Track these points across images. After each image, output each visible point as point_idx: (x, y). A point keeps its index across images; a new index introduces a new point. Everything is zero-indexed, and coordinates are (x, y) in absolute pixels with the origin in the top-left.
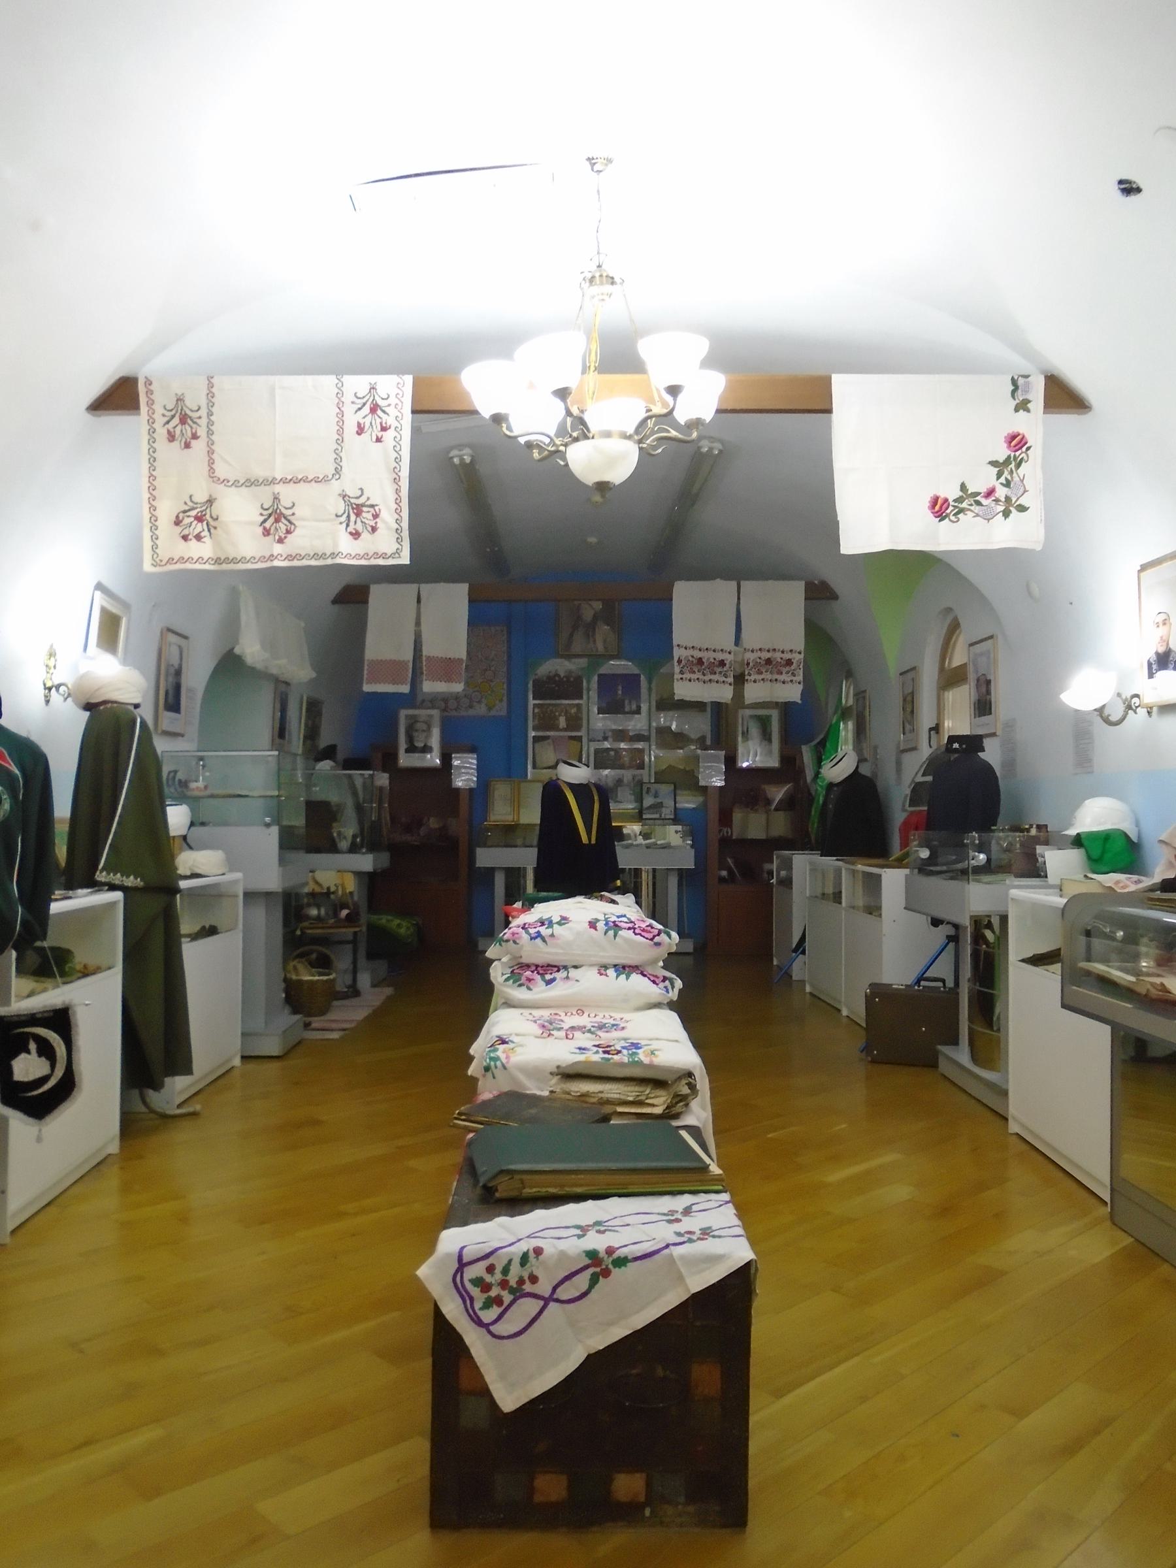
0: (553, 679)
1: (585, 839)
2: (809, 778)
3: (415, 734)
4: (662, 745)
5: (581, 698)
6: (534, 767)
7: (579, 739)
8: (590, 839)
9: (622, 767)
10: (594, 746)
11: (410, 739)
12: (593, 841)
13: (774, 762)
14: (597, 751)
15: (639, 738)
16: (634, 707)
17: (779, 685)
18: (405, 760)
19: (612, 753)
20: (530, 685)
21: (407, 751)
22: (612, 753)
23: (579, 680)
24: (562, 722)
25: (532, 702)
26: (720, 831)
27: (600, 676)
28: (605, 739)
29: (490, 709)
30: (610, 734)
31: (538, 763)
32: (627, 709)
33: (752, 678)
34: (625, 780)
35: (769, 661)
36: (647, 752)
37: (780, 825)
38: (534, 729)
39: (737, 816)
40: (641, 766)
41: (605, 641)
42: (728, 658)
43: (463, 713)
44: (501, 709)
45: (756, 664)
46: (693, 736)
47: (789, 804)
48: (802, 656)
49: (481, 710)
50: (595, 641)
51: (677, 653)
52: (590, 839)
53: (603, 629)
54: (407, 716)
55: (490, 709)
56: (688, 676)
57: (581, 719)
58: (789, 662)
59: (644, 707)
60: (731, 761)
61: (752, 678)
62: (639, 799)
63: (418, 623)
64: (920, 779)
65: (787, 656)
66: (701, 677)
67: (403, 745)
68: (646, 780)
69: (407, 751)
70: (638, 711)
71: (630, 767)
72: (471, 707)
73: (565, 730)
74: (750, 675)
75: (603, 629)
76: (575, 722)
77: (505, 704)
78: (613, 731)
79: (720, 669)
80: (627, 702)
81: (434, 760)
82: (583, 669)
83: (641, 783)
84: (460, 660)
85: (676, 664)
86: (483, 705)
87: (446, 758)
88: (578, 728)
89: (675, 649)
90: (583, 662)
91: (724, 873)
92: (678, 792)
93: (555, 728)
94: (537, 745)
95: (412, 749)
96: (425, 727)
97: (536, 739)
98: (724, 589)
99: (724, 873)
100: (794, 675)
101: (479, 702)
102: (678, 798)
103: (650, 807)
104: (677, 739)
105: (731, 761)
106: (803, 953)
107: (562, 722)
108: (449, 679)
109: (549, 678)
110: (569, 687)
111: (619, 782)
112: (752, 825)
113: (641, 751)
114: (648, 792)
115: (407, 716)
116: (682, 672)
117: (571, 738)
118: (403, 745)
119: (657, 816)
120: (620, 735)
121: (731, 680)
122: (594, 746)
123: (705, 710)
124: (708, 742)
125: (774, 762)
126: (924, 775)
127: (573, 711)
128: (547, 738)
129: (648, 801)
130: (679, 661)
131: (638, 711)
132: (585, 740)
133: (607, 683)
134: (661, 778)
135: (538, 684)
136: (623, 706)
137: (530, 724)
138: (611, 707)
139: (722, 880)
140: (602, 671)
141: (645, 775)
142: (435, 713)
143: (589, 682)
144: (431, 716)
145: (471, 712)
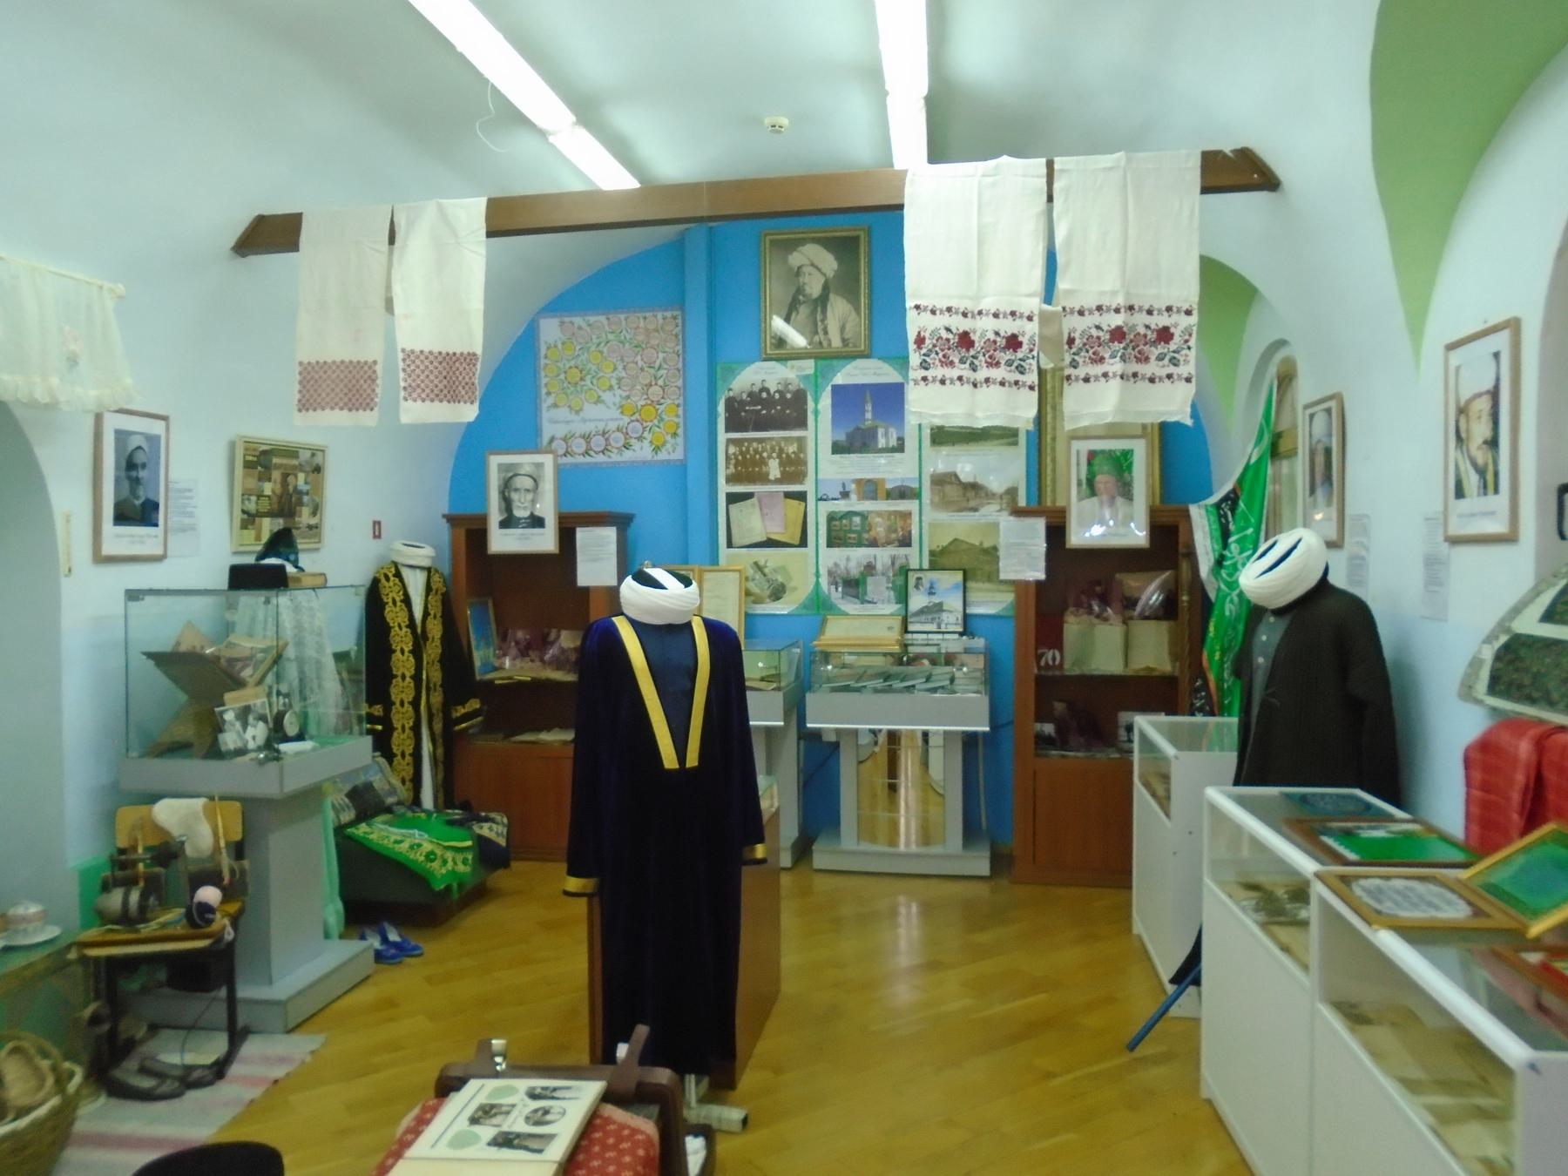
0: (757, 396)
1: (669, 759)
2: (1204, 569)
3: (514, 496)
4: (944, 504)
5: (801, 423)
6: (730, 545)
7: (801, 496)
9: (873, 543)
10: (826, 508)
11: (507, 504)
12: (692, 760)
13: (1137, 535)
14: (831, 518)
15: (903, 493)
16: (893, 442)
17: (1144, 385)
18: (502, 542)
19: (857, 520)
20: (721, 408)
21: (505, 524)
22: (857, 520)
23: (800, 397)
24: (774, 469)
25: (722, 436)
26: (1039, 657)
27: (837, 390)
28: (845, 495)
29: (657, 449)
30: (853, 486)
31: (736, 540)
32: (882, 442)
33: (1081, 372)
34: (879, 567)
35: (1118, 334)
36: (915, 518)
37: (1152, 650)
38: (729, 480)
39: (1073, 626)
40: (906, 542)
41: (842, 329)
42: (1029, 331)
43: (615, 457)
44: (673, 452)
45: (1092, 342)
46: (996, 484)
47: (1168, 609)
48: (1194, 319)
49: (642, 452)
50: (826, 332)
51: (914, 324)
53: (838, 307)
54: (500, 465)
55: (657, 449)
56: (938, 372)
57: (805, 464)
58: (1165, 335)
59: (911, 444)
60: (1056, 533)
61: (1081, 372)
62: (903, 598)
63: (388, 287)
64: (1530, 624)
65: (1160, 321)
66: (967, 373)
67: (495, 518)
68: (914, 564)
69: (505, 524)
70: (900, 448)
71: (888, 543)
72: (627, 446)
73: (778, 481)
74: (1074, 364)
75: (838, 307)
76: (794, 469)
77: (680, 440)
78: (859, 482)
79: (1009, 355)
80: (881, 431)
81: (545, 541)
82: (807, 377)
83: (905, 571)
84: (471, 358)
85: (912, 346)
86: (646, 442)
87: (567, 536)
88: (799, 477)
89: (911, 315)
90: (809, 366)
91: (1049, 728)
92: (970, 584)
93: (763, 479)
94: (734, 508)
95: (508, 522)
96: (528, 483)
97: (733, 499)
98: (1017, 175)
99: (1049, 728)
100: (1174, 362)
101: (640, 439)
102: (972, 597)
103: (922, 612)
104: (972, 493)
105: (1056, 533)
106: (1197, 982)
107: (774, 469)
108: (454, 397)
109: (750, 394)
110: (786, 411)
111: (870, 568)
112: (1102, 646)
113: (906, 516)
114: (917, 587)
115: (500, 465)
116: (925, 366)
117: (788, 495)
118: (495, 518)
119: (933, 627)
120: (870, 489)
121: (1032, 378)
122: (826, 508)
123: (1015, 444)
124: (1022, 503)
125: (1137, 535)
126: (1549, 616)
127: (792, 449)
128: (749, 496)
129: (918, 601)
130: (920, 341)
131: (900, 448)
132: (811, 498)
133: (846, 398)
134: (939, 560)
135: (731, 404)
136: (874, 437)
138: (855, 442)
139: (1042, 741)
140: (840, 379)
141: (914, 557)
142: (547, 460)
143: (816, 402)
144: (539, 466)
145: (628, 455)
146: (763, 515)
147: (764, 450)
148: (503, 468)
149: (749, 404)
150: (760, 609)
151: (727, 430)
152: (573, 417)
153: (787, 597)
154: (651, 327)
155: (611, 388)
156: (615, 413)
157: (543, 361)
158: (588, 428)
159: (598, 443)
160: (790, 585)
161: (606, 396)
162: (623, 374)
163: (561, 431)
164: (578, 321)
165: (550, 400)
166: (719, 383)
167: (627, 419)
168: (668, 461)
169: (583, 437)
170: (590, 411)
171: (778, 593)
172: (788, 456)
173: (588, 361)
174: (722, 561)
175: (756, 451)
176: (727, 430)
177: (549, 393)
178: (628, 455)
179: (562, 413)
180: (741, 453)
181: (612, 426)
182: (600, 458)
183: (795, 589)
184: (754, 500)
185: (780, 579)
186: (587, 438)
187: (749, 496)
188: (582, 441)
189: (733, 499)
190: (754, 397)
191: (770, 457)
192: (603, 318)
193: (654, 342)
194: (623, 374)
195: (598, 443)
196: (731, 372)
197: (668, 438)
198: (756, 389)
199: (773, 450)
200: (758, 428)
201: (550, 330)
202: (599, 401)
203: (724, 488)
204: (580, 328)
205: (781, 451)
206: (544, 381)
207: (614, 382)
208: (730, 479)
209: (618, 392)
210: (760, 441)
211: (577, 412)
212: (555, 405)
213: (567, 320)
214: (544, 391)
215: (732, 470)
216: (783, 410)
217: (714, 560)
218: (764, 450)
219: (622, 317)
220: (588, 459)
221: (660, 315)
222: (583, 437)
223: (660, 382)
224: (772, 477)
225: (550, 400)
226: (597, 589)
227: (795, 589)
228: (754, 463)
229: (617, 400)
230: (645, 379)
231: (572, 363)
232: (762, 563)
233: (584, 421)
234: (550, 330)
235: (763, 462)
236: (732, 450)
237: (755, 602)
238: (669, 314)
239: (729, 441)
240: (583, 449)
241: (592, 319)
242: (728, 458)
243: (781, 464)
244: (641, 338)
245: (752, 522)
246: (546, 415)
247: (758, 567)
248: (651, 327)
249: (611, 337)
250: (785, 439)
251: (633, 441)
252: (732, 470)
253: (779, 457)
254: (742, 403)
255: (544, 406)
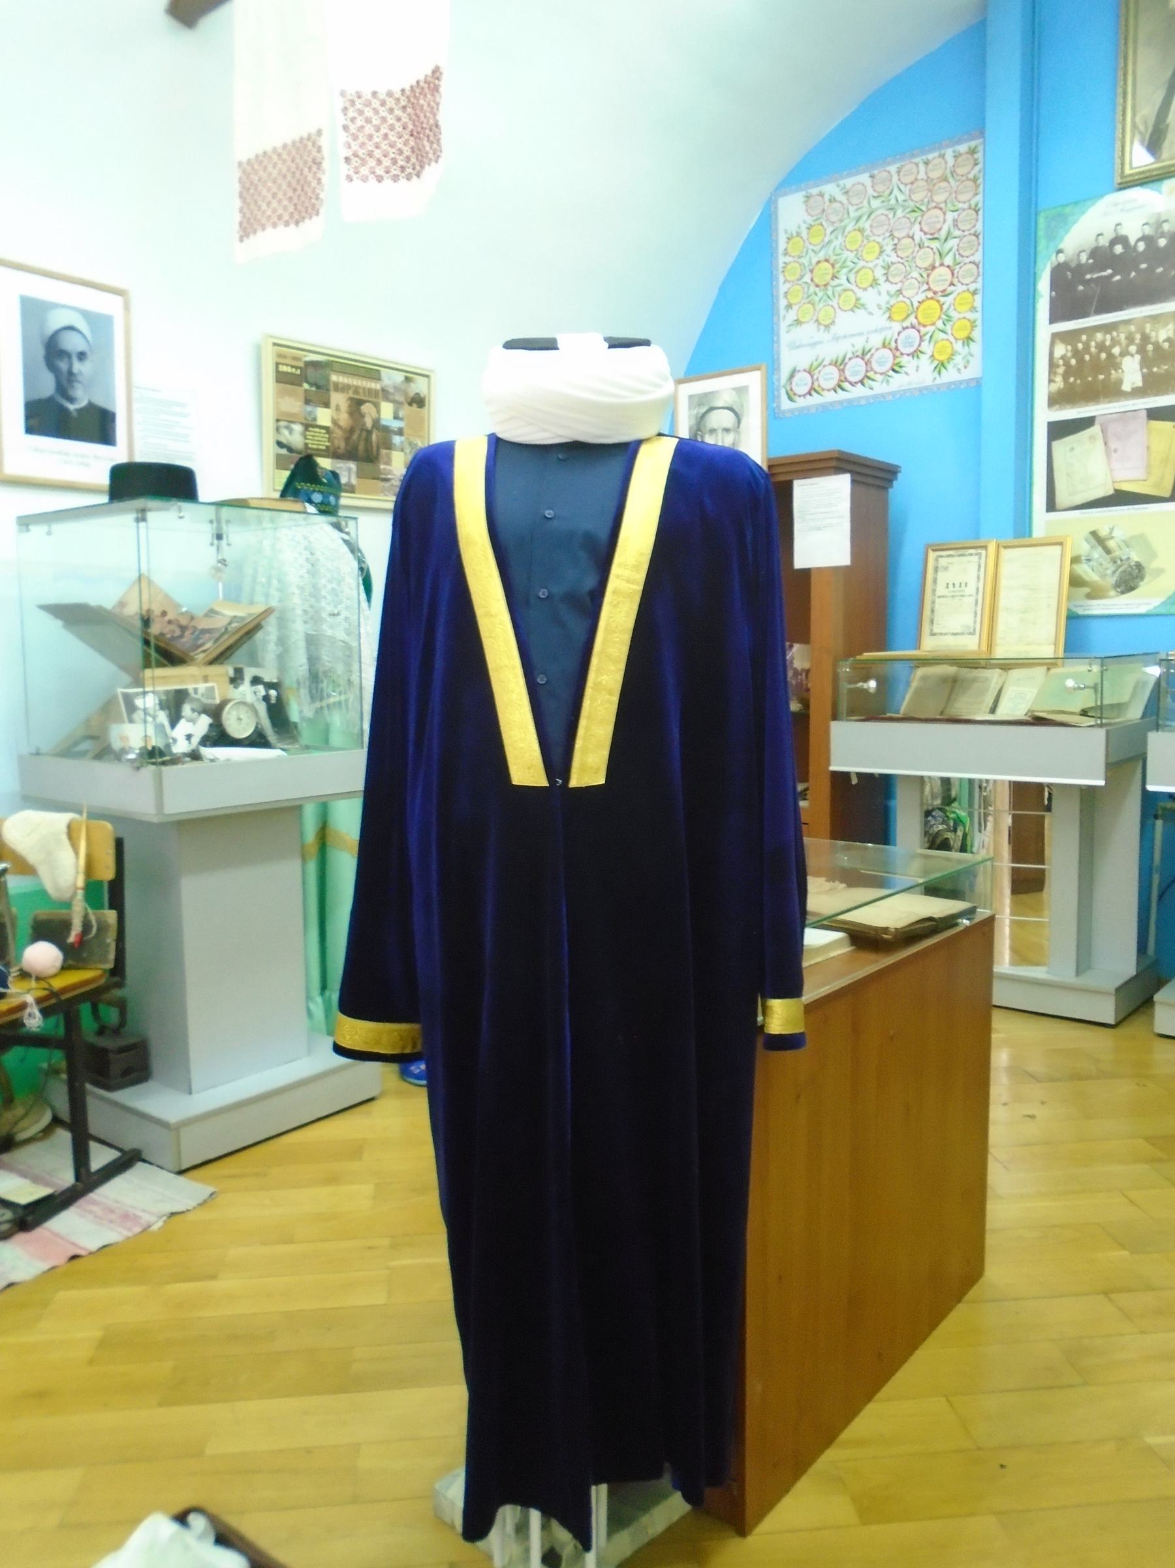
1: (525, 763)
6: (1051, 506)
8: (557, 747)
12: (590, 765)
24: (1131, 373)
25: (1044, 329)
38: (1055, 400)
43: (879, 387)
44: (968, 365)
49: (919, 373)
52: (557, 747)
54: (691, 397)
73: (1137, 393)
77: (976, 348)
86: (924, 359)
93: (1113, 391)
96: (727, 419)
97: (1058, 430)
101: (916, 354)
107: (1131, 373)
109: (1095, 253)
115: (691, 397)
128: (1088, 422)
135: (1058, 273)
137: (1042, 388)
144: (741, 391)
145: (898, 382)
146: (1108, 452)
147: (1115, 342)
148: (699, 400)
149: (1092, 269)
150: (1097, 607)
151: (1053, 319)
152: (823, 335)
153: (1144, 587)
154: (935, 175)
155: (875, 283)
156: (880, 320)
157: (782, 259)
158: (842, 348)
159: (856, 369)
160: (1151, 566)
161: (870, 298)
162: (894, 258)
163: (804, 359)
164: (830, 189)
165: (792, 315)
166: (1042, 244)
167: (897, 327)
168: (957, 384)
169: (835, 363)
170: (847, 322)
171: (1130, 579)
172: (1157, 347)
173: (844, 248)
174: (1038, 532)
175: (1101, 347)
176: (1053, 319)
177: (789, 306)
178: (898, 382)
179: (808, 331)
180: (1076, 353)
181: (876, 341)
182: (859, 391)
183: (1160, 572)
184: (1095, 430)
185: (1135, 557)
186: (840, 364)
187: (1088, 422)
188: (834, 370)
189: (1058, 430)
190: (1101, 256)
191: (1124, 354)
192: (864, 178)
193: (939, 198)
194: (894, 258)
195: (856, 369)
196: (1062, 221)
197: (958, 346)
198: (1104, 242)
199: (1130, 339)
200: (1103, 308)
201: (792, 211)
202: (858, 305)
203: (1043, 415)
204: (833, 200)
205: (1145, 339)
206: (783, 288)
207: (879, 273)
208: (1055, 400)
209: (885, 287)
210: (1107, 328)
211: (827, 327)
212: (798, 322)
213: (814, 191)
214: (783, 303)
215: (1059, 383)
216: (1151, 269)
217: (1022, 531)
218: (1115, 342)
219: (893, 169)
220: (841, 395)
221: (949, 153)
222: (835, 363)
223: (948, 260)
224: (1126, 387)
225: (792, 315)
226: (820, 570)
227: (1160, 572)
228: (1097, 367)
229: (885, 297)
230: (925, 259)
231: (821, 256)
232: (1103, 533)
233: (836, 338)
234: (792, 211)
235: (1113, 363)
236: (1060, 350)
237: (1089, 596)
238: (963, 148)
239: (1056, 337)
240: (833, 383)
241: (848, 182)
242: (1052, 365)
243: (1145, 363)
244: (917, 197)
245: (1088, 466)
246: (785, 338)
247: (1097, 538)
248: (935, 175)
249: (875, 203)
250: (1155, 319)
251: (905, 360)
252: (1059, 383)
253: (1142, 350)
254: (1080, 270)
255: (783, 326)
